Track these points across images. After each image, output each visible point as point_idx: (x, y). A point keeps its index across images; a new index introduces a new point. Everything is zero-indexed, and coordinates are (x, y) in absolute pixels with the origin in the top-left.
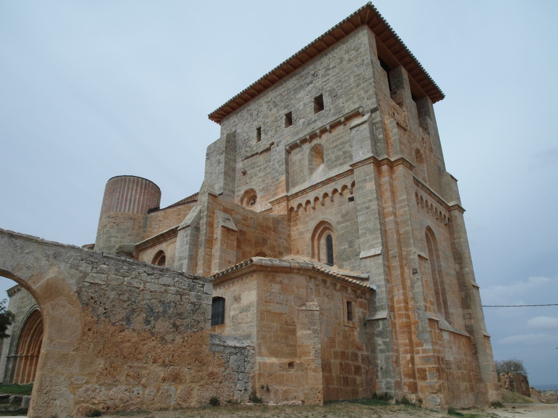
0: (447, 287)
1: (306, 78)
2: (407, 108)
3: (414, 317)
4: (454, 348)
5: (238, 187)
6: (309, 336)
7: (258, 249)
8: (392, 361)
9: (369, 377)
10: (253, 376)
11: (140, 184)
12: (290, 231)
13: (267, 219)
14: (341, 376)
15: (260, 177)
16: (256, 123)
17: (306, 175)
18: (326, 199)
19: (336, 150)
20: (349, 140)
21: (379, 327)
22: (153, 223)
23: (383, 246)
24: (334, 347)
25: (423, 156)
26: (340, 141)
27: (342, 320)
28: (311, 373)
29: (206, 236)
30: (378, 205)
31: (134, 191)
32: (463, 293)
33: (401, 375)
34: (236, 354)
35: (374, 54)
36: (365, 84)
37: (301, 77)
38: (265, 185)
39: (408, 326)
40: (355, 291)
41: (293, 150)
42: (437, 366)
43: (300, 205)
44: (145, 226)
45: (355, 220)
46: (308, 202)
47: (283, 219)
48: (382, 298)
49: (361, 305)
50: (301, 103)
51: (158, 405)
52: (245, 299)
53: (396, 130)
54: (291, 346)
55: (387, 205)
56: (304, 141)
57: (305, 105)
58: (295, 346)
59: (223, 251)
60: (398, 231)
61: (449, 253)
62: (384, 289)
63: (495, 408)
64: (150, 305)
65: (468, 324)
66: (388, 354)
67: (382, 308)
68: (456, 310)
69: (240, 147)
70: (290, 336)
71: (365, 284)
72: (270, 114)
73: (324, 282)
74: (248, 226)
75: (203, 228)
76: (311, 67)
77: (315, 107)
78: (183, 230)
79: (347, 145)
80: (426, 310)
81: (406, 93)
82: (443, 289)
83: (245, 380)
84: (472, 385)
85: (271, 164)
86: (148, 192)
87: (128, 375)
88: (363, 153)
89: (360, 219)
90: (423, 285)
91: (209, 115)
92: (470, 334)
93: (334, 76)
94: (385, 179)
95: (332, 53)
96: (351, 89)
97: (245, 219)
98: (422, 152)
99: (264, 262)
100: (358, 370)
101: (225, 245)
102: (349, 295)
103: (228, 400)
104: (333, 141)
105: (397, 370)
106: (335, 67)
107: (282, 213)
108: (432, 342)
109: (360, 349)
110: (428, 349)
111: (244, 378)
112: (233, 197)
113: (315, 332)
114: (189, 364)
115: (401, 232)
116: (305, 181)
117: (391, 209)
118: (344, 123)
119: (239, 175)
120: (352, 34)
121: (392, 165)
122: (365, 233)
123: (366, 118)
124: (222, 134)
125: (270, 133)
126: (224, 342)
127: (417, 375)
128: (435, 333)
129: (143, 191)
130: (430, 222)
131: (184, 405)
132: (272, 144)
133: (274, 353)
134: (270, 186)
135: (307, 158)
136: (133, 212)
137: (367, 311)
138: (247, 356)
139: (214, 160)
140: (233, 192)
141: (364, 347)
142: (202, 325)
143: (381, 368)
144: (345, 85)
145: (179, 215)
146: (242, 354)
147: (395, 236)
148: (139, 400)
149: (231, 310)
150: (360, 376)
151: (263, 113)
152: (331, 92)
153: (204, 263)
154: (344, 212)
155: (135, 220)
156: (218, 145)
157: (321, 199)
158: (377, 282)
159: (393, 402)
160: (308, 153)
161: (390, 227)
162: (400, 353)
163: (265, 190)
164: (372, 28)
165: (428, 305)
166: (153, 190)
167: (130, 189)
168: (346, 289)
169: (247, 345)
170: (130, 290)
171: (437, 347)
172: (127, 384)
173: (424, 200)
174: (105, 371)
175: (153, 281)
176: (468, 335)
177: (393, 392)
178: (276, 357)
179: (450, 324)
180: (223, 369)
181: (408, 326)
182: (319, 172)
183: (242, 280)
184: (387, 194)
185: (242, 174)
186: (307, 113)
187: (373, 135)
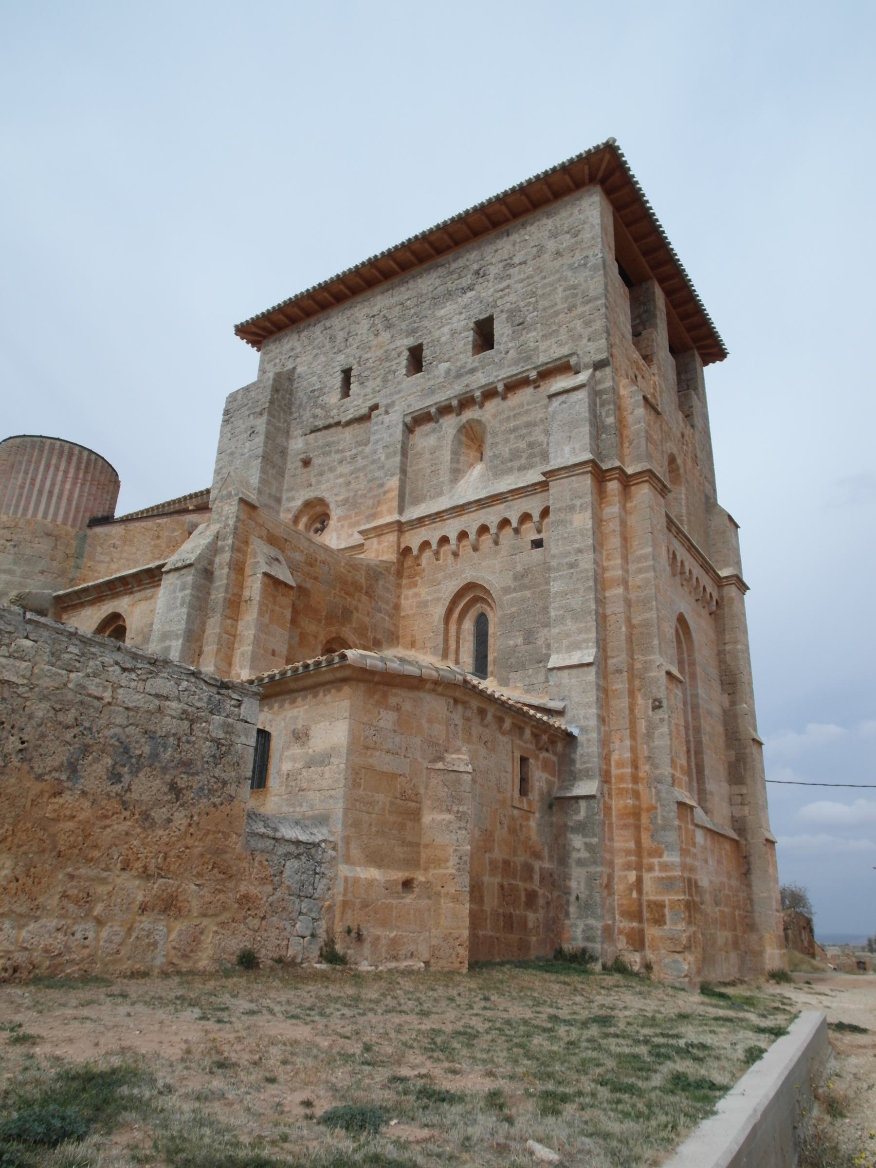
0: (705, 739)
1: (460, 277)
2: (659, 368)
3: (648, 797)
4: (710, 862)
5: (288, 490)
6: (447, 827)
7: (333, 629)
8: (601, 885)
9: (551, 914)
10: (330, 907)
11: (75, 458)
12: (399, 597)
13: (354, 567)
14: (501, 911)
15: (341, 475)
16: (341, 357)
17: (443, 482)
18: (484, 537)
19: (512, 436)
20: (542, 420)
21: (577, 812)
22: (99, 549)
23: (598, 647)
24: (491, 850)
25: (682, 471)
26: (525, 419)
27: (509, 795)
28: (446, 905)
29: (226, 591)
30: (595, 562)
31: (61, 474)
32: (733, 753)
33: (614, 913)
34: (298, 857)
35: (610, 248)
36: (587, 308)
37: (451, 273)
38: (351, 494)
39: (636, 814)
40: (536, 736)
41: (420, 425)
42: (687, 897)
43: (426, 545)
44: (79, 555)
45: (543, 588)
46: (444, 540)
47: (387, 569)
48: (588, 754)
50: (446, 329)
51: (126, 966)
52: (320, 737)
53: (641, 411)
54: (410, 844)
55: (611, 563)
56: (445, 410)
57: (454, 333)
58: (418, 845)
59: (262, 628)
60: (629, 619)
61: (713, 672)
62: (595, 735)
63: (778, 983)
64: (123, 738)
65: (737, 815)
66: (592, 869)
67: (588, 775)
68: (717, 786)
69: (300, 405)
70: (409, 824)
71: (557, 722)
72: (375, 342)
73: (482, 712)
74: (316, 578)
75: (222, 573)
76: (474, 255)
77: (475, 341)
78: (176, 574)
79: (538, 430)
80: (673, 785)
81: (660, 337)
82: (699, 743)
83: (313, 915)
84: (736, 936)
85: (367, 450)
86: (93, 479)
87: (65, 896)
88: (572, 450)
89: (556, 587)
90: (670, 734)
91: (236, 327)
92: (740, 835)
93: (521, 281)
94: (612, 510)
95: (522, 232)
96: (557, 313)
97: (311, 562)
98: (679, 461)
99: (369, 661)
100: (531, 897)
101: (267, 616)
102: (526, 742)
103: (276, 956)
104: (509, 418)
105: (608, 902)
106: (525, 263)
107: (385, 558)
108: (681, 849)
109: (537, 856)
110: (673, 864)
111: (311, 910)
112: (278, 512)
113: (460, 819)
114: (199, 875)
115: (635, 621)
116: (440, 494)
117: (619, 572)
118: (535, 383)
119: (293, 464)
120: (566, 198)
121: (627, 481)
122: (563, 618)
123: (582, 377)
124: (262, 371)
125: (370, 384)
126: (275, 830)
127: (646, 915)
128: (687, 830)
129: (81, 475)
130: (685, 605)
131: (185, 966)
132: (375, 407)
133: (374, 859)
134: (364, 496)
135: (449, 448)
136: (54, 520)
137: (556, 780)
138: (320, 863)
139: (241, 425)
140: (278, 500)
141: (546, 853)
142: (231, 789)
143: (577, 898)
144: (543, 303)
145: (158, 537)
146: (311, 857)
147: (624, 629)
148: (86, 952)
149: (284, 761)
150: (536, 911)
151: (359, 337)
152: (512, 314)
153: (219, 650)
154: (519, 568)
155: (57, 538)
156: (253, 394)
157: (472, 536)
158: (581, 720)
159: (598, 967)
160: (451, 437)
161: (615, 609)
162: (616, 868)
163: (350, 503)
164: (609, 192)
165: (678, 774)
166: (101, 475)
167: (52, 469)
168: (521, 730)
169: (321, 838)
170: (82, 703)
171: (688, 860)
172: (63, 917)
173: (679, 559)
174: (14, 885)
175: (133, 684)
176: (735, 836)
177: (598, 946)
178: (379, 867)
179: (706, 813)
180: (269, 888)
181: (636, 814)
182: (472, 479)
183: (315, 696)
184: (615, 542)
185: (300, 464)
186: (456, 351)
187: (595, 416)
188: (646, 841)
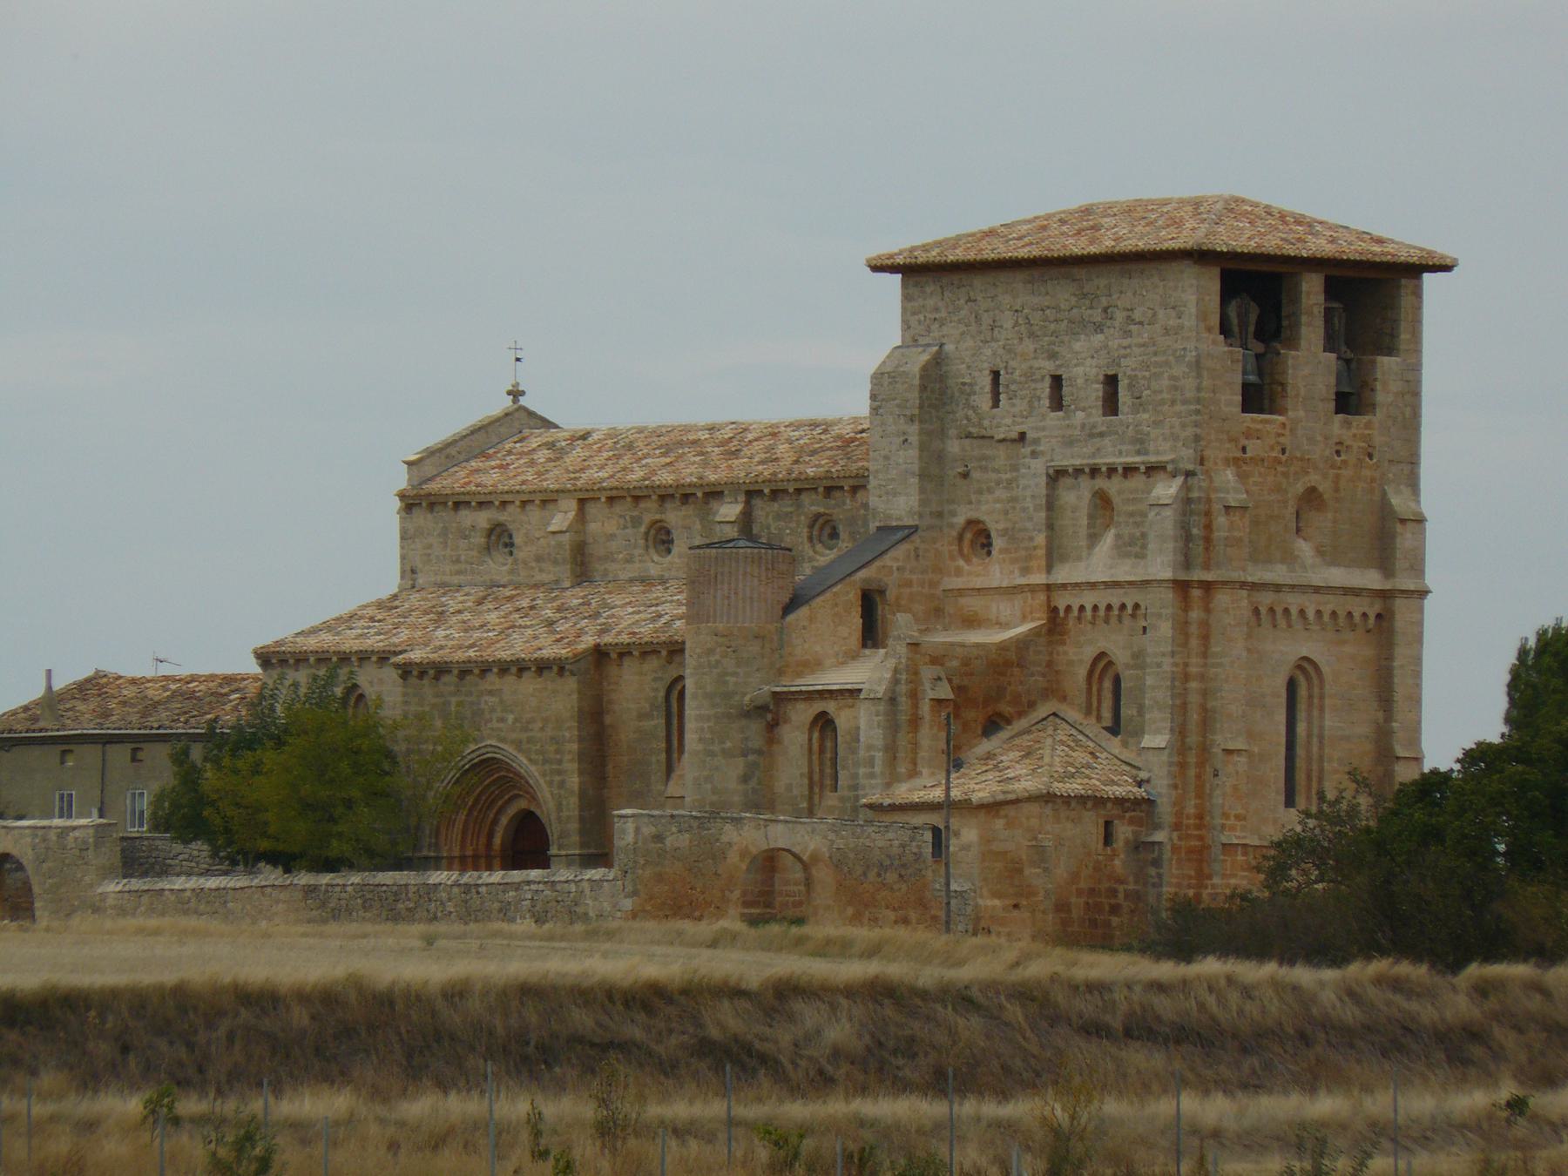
15: (998, 501)
49: (1131, 821)
56: (1078, 471)
82: (1321, 770)
94: (1195, 615)
109: (1122, 882)
133: (996, 894)
141: (1131, 879)
155: (763, 638)
188: (1206, 871)
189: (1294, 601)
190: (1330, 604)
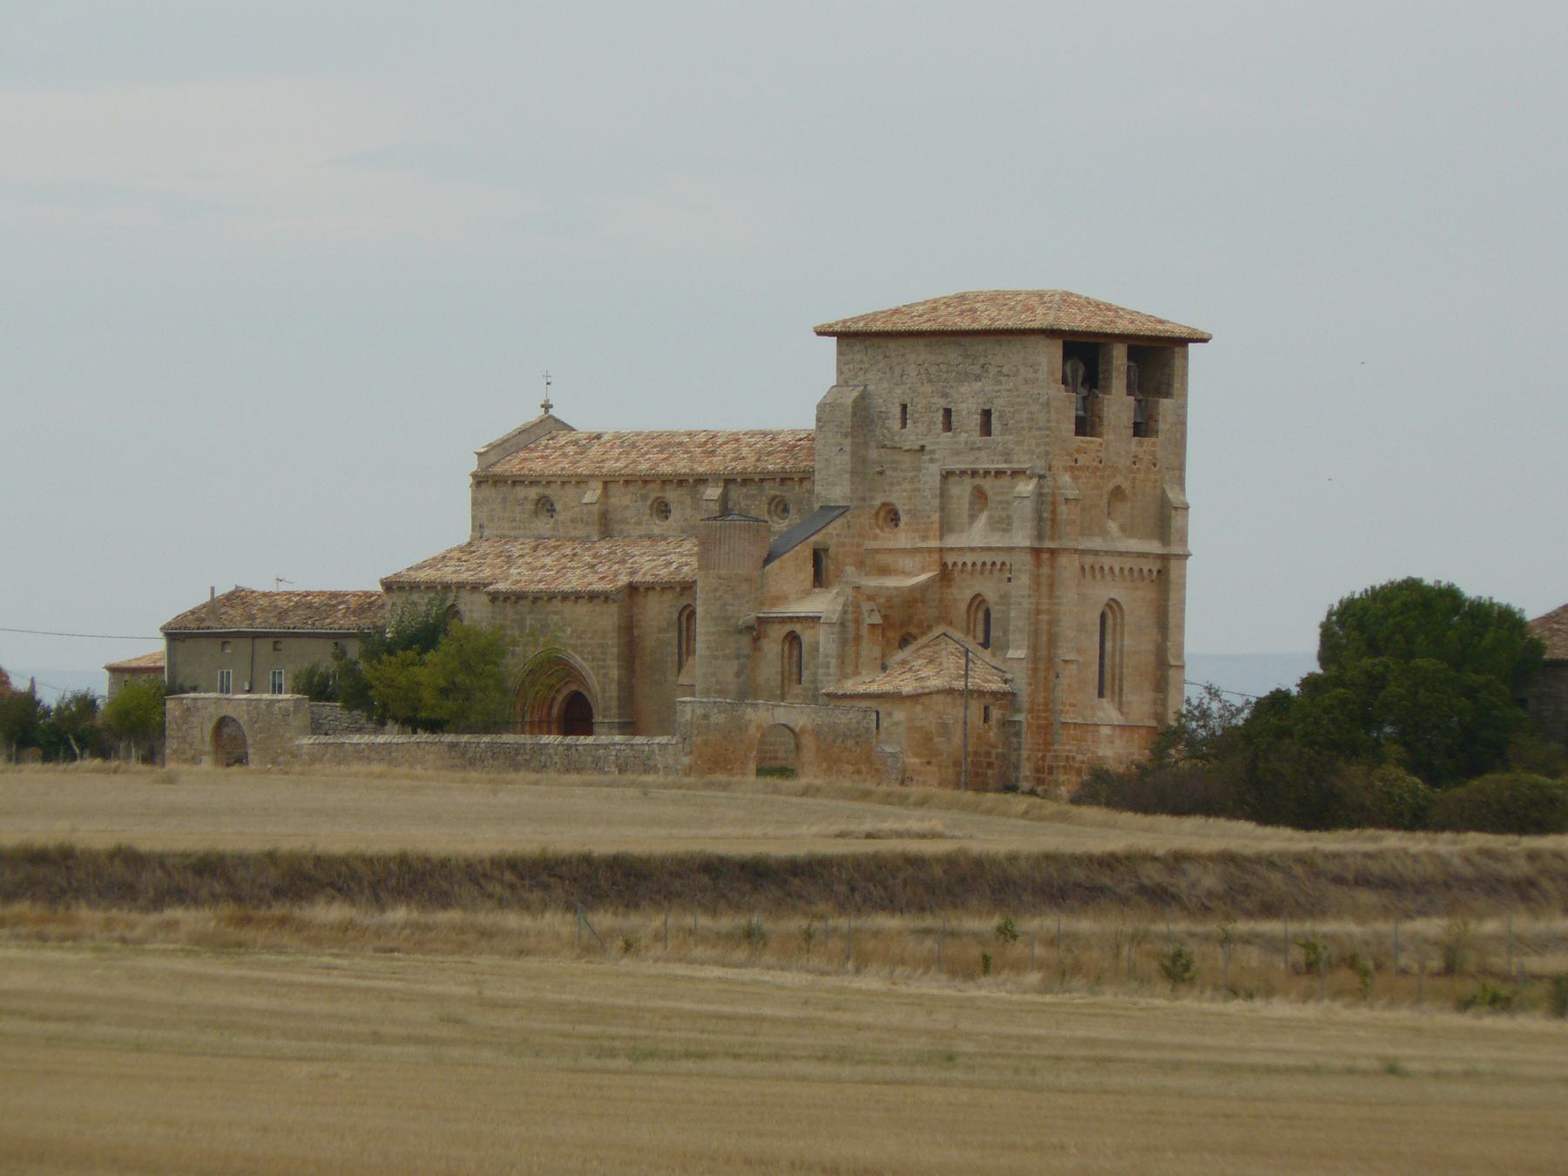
4: (1117, 742)
49: (1001, 707)
82: (1121, 673)
94: (1045, 570)
133: (916, 755)
189: (1106, 562)
190: (1129, 563)
